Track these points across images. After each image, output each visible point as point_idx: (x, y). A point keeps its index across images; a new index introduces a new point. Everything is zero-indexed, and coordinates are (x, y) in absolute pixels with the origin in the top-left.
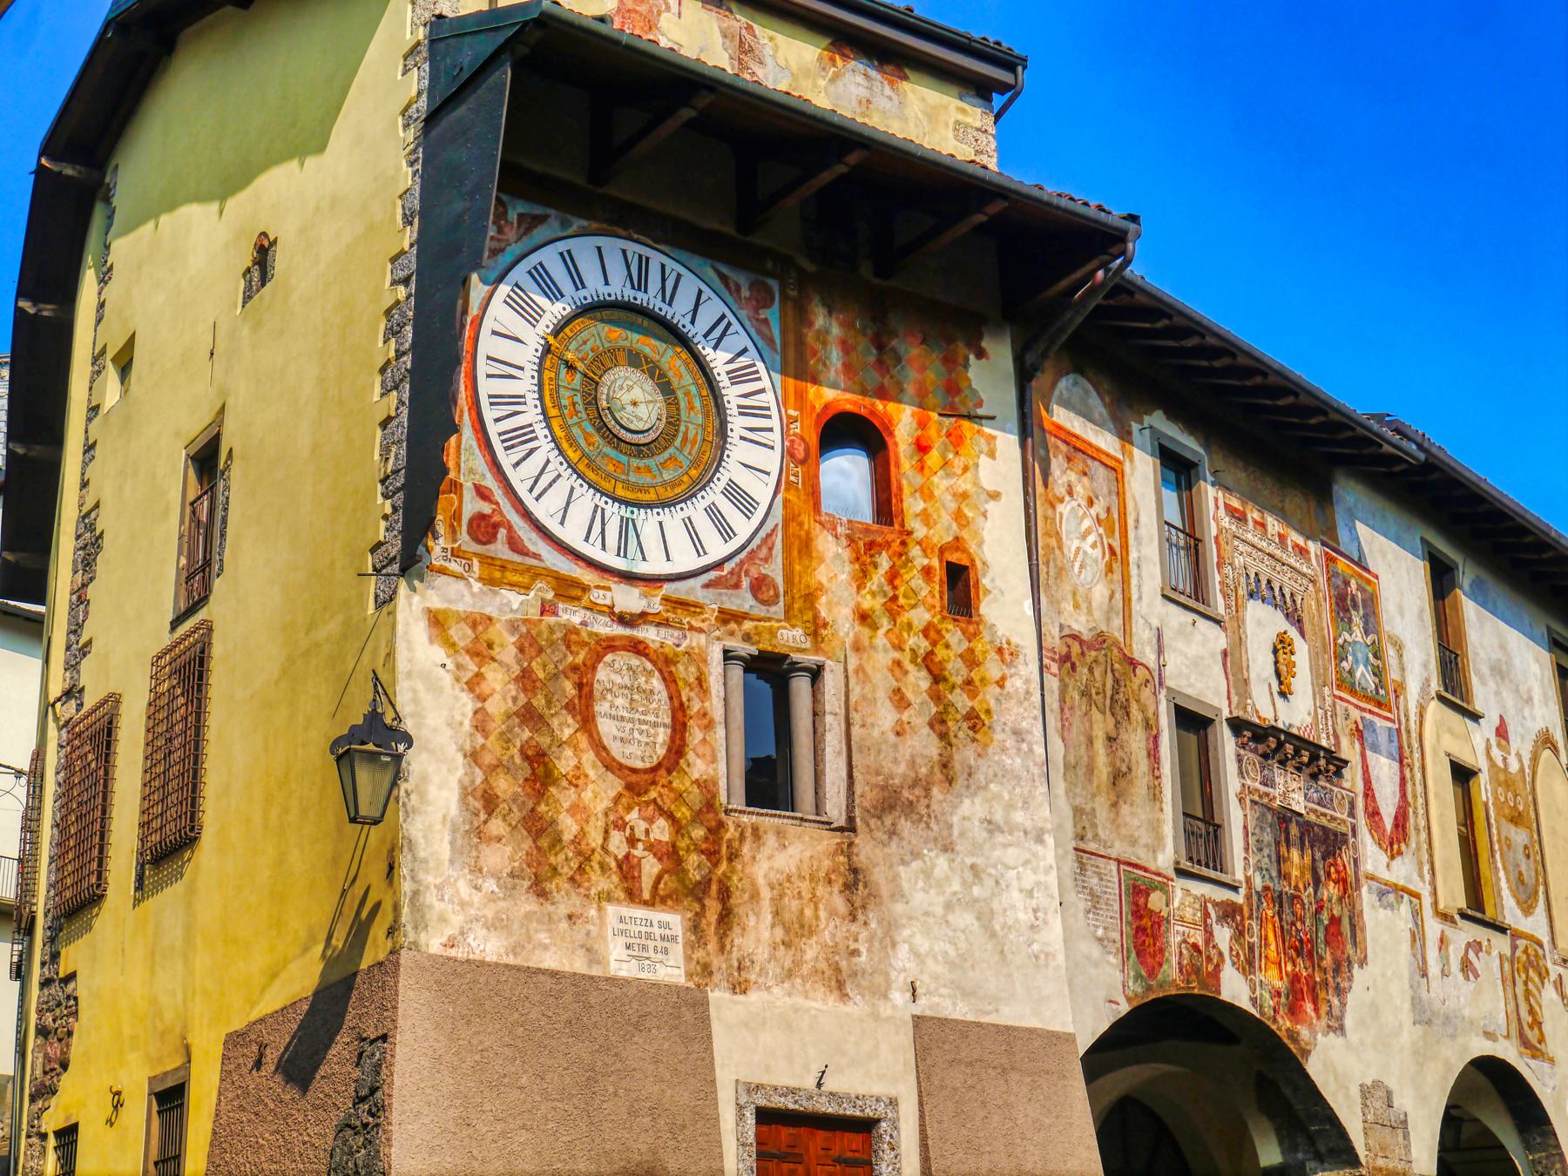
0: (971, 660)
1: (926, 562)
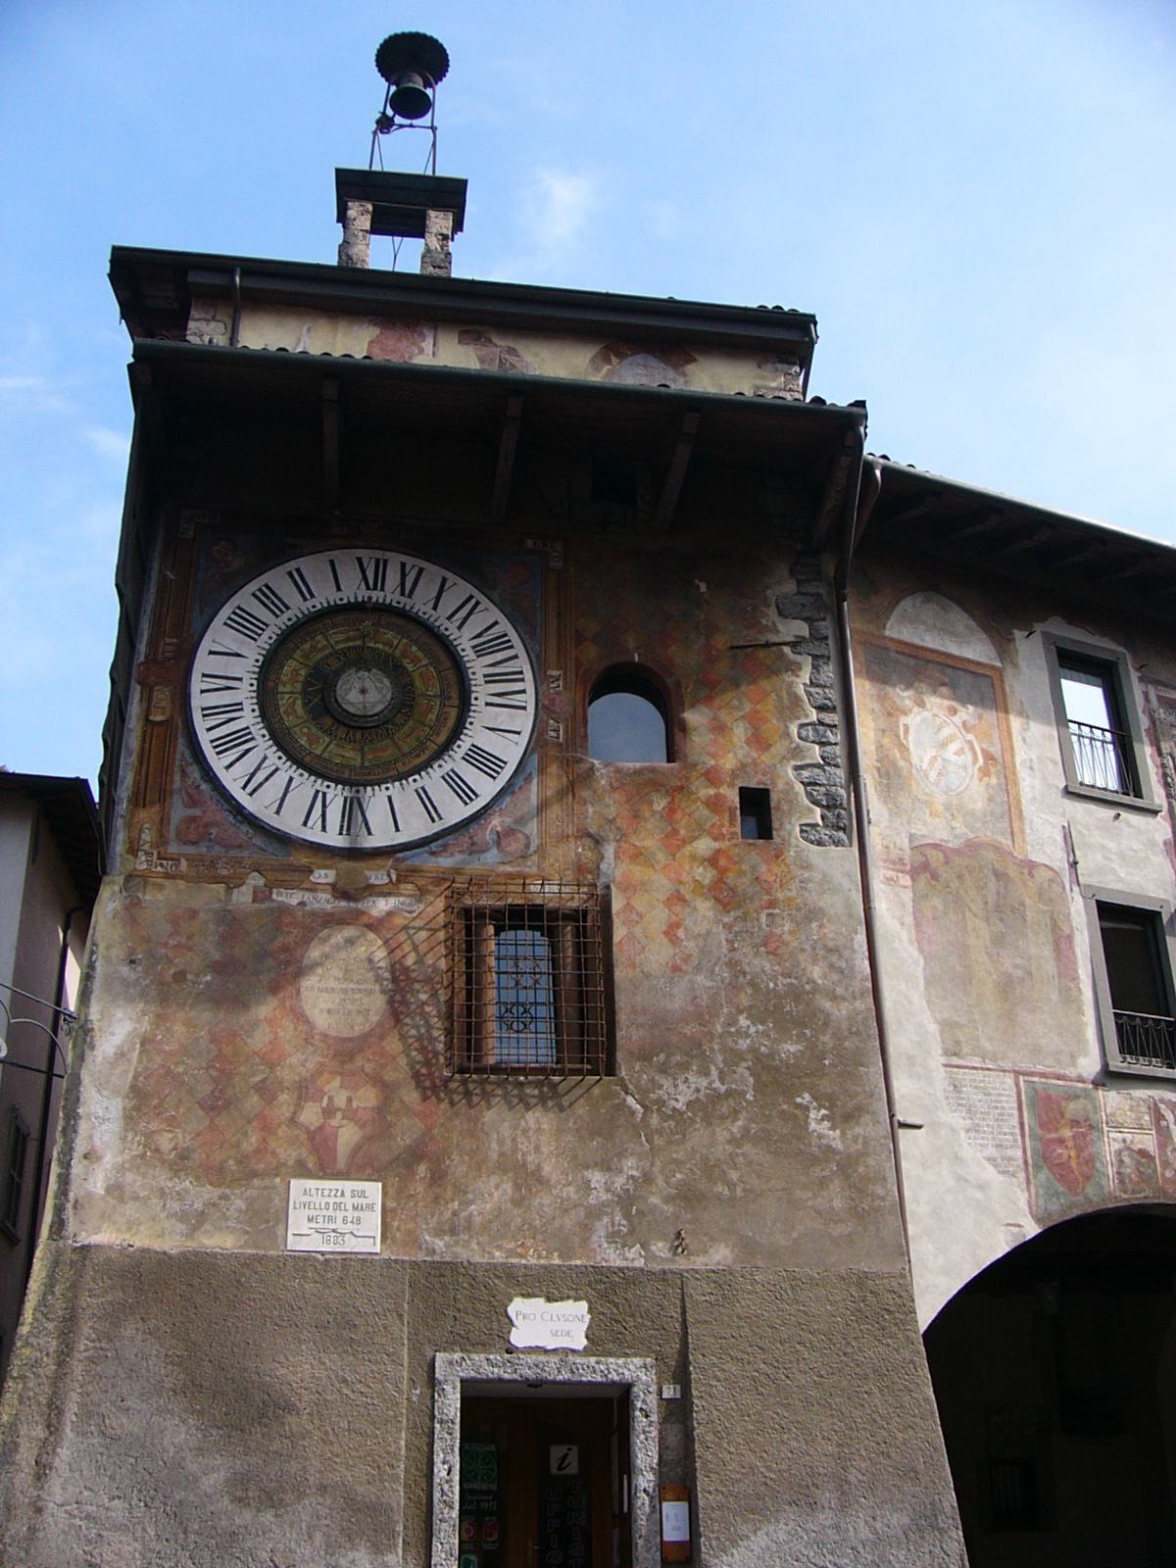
1: (712, 792)
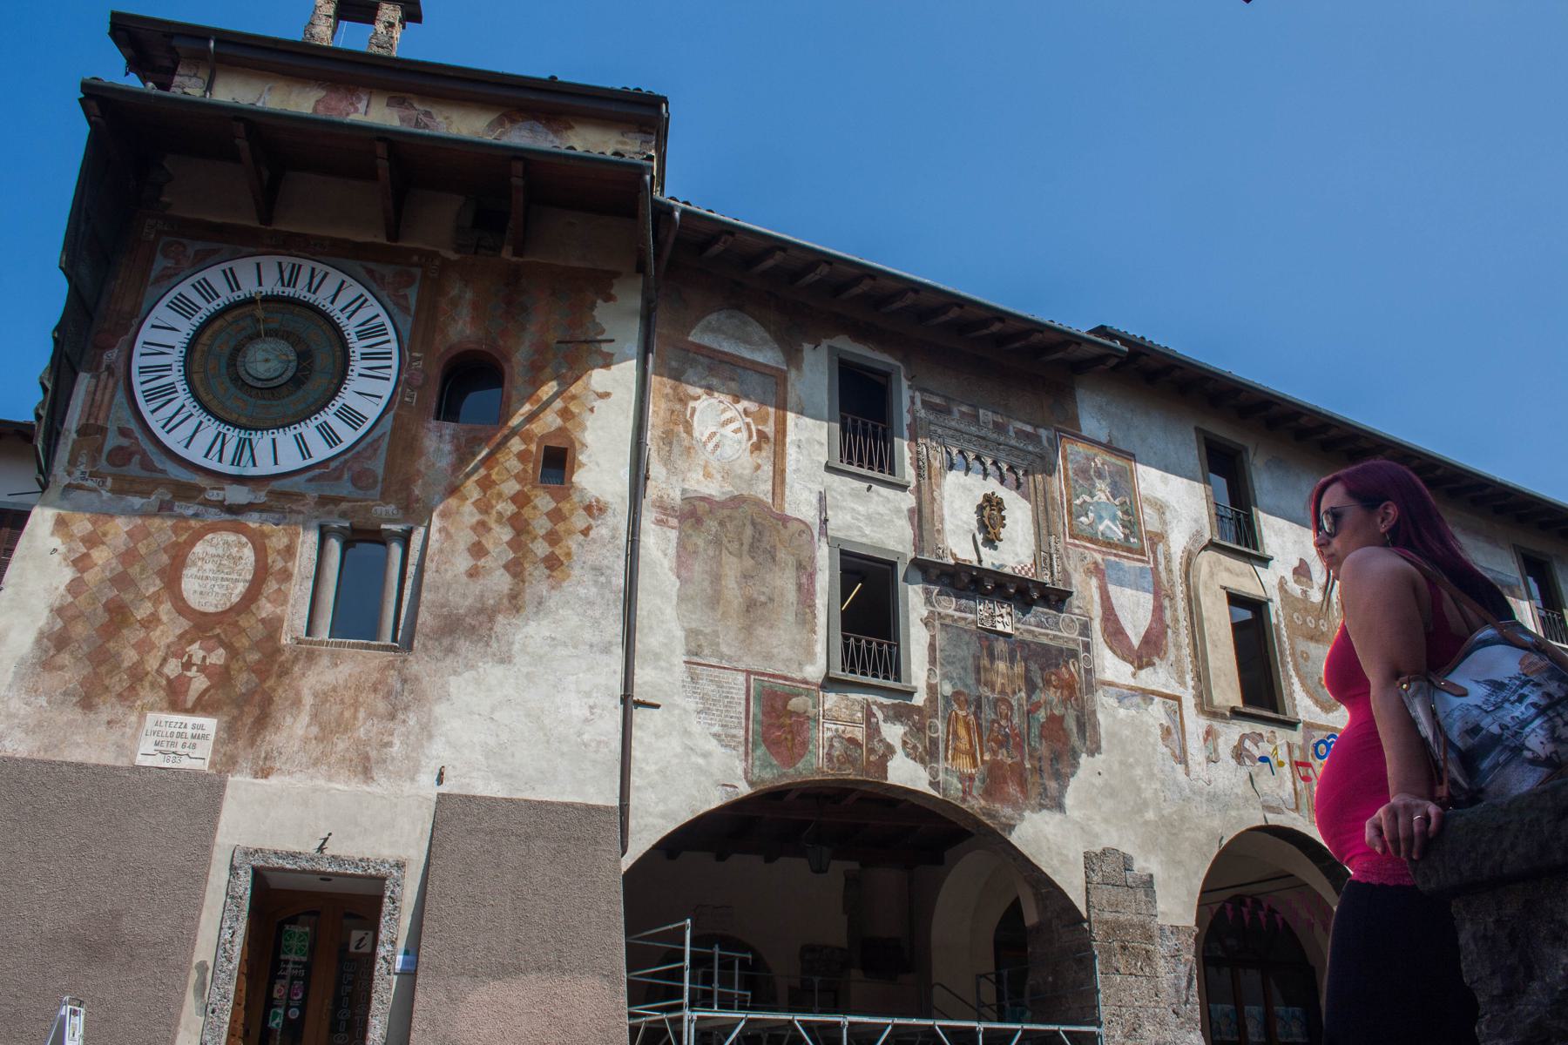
0: (556, 516)
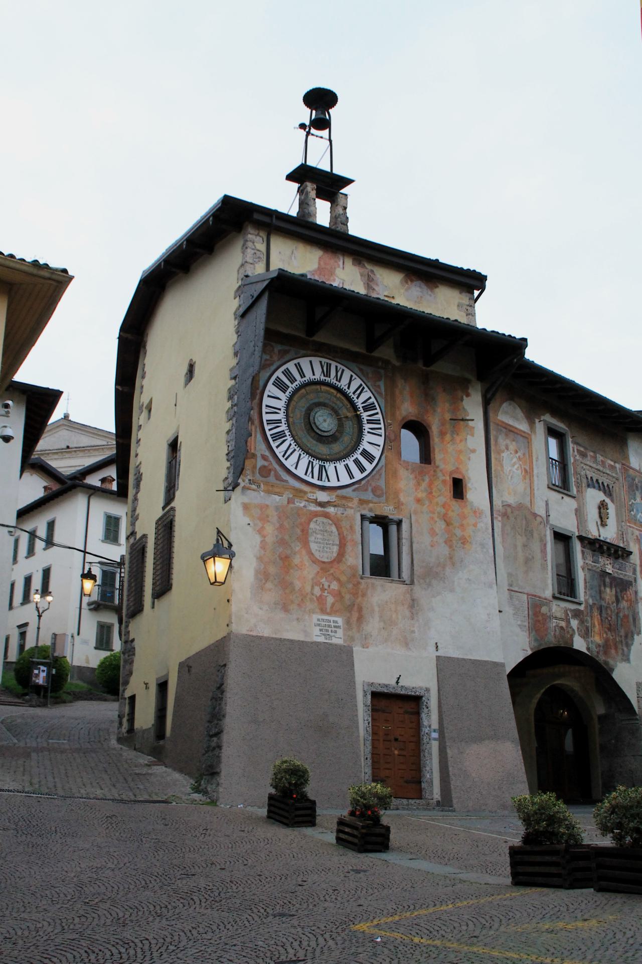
0: (463, 517)
